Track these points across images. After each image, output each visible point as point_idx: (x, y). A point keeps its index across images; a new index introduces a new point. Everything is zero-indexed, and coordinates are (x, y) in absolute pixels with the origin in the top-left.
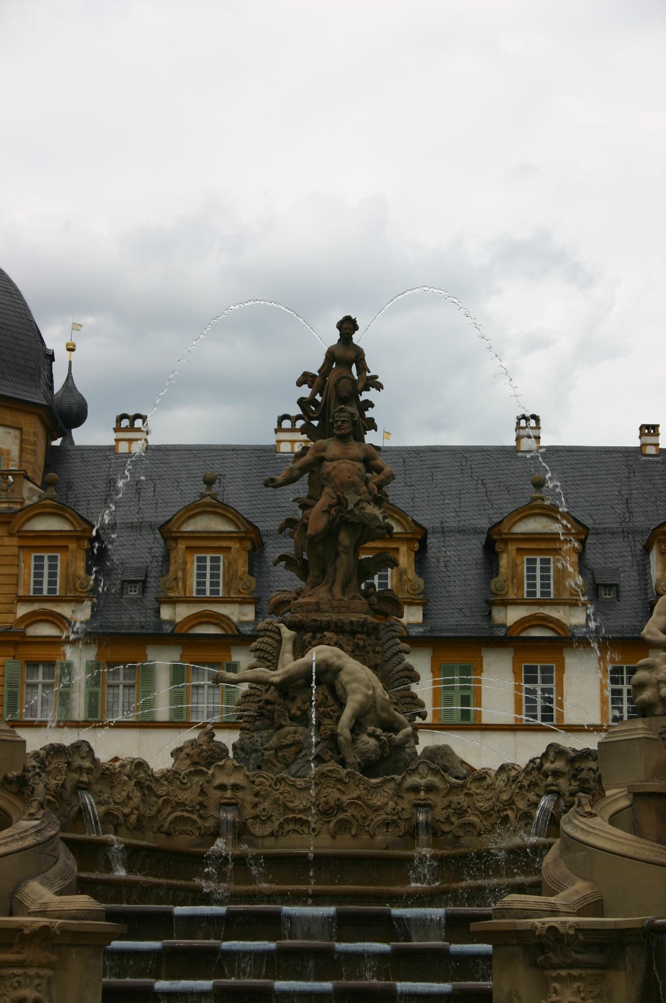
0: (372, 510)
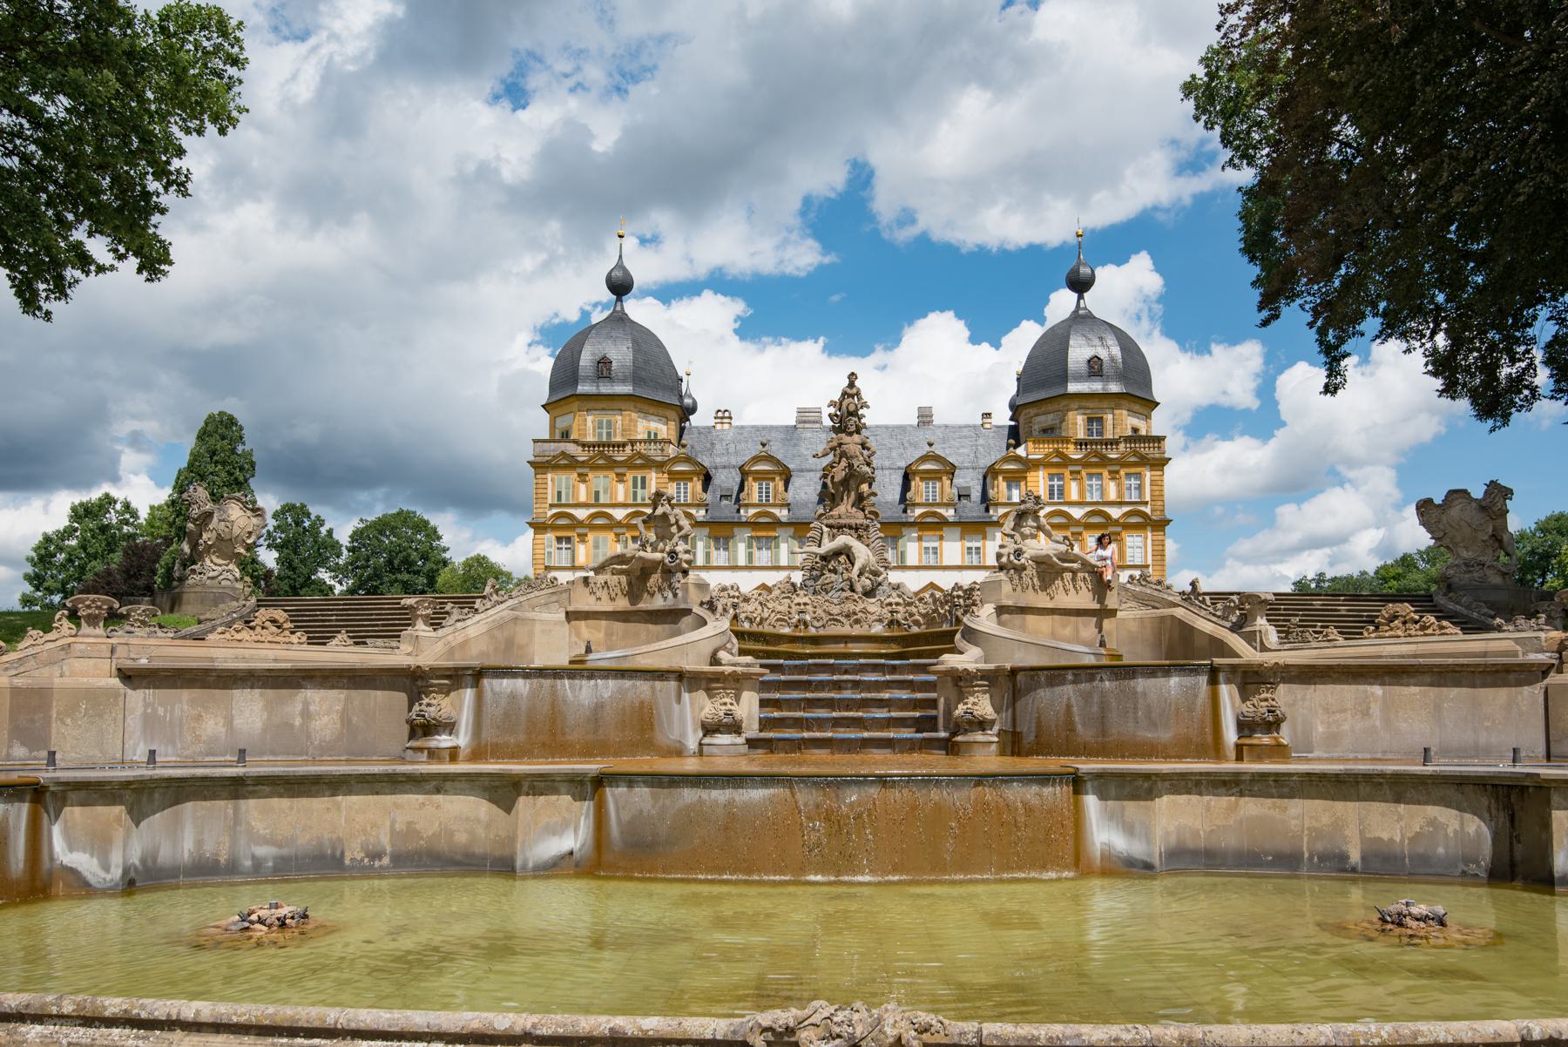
0: (866, 469)
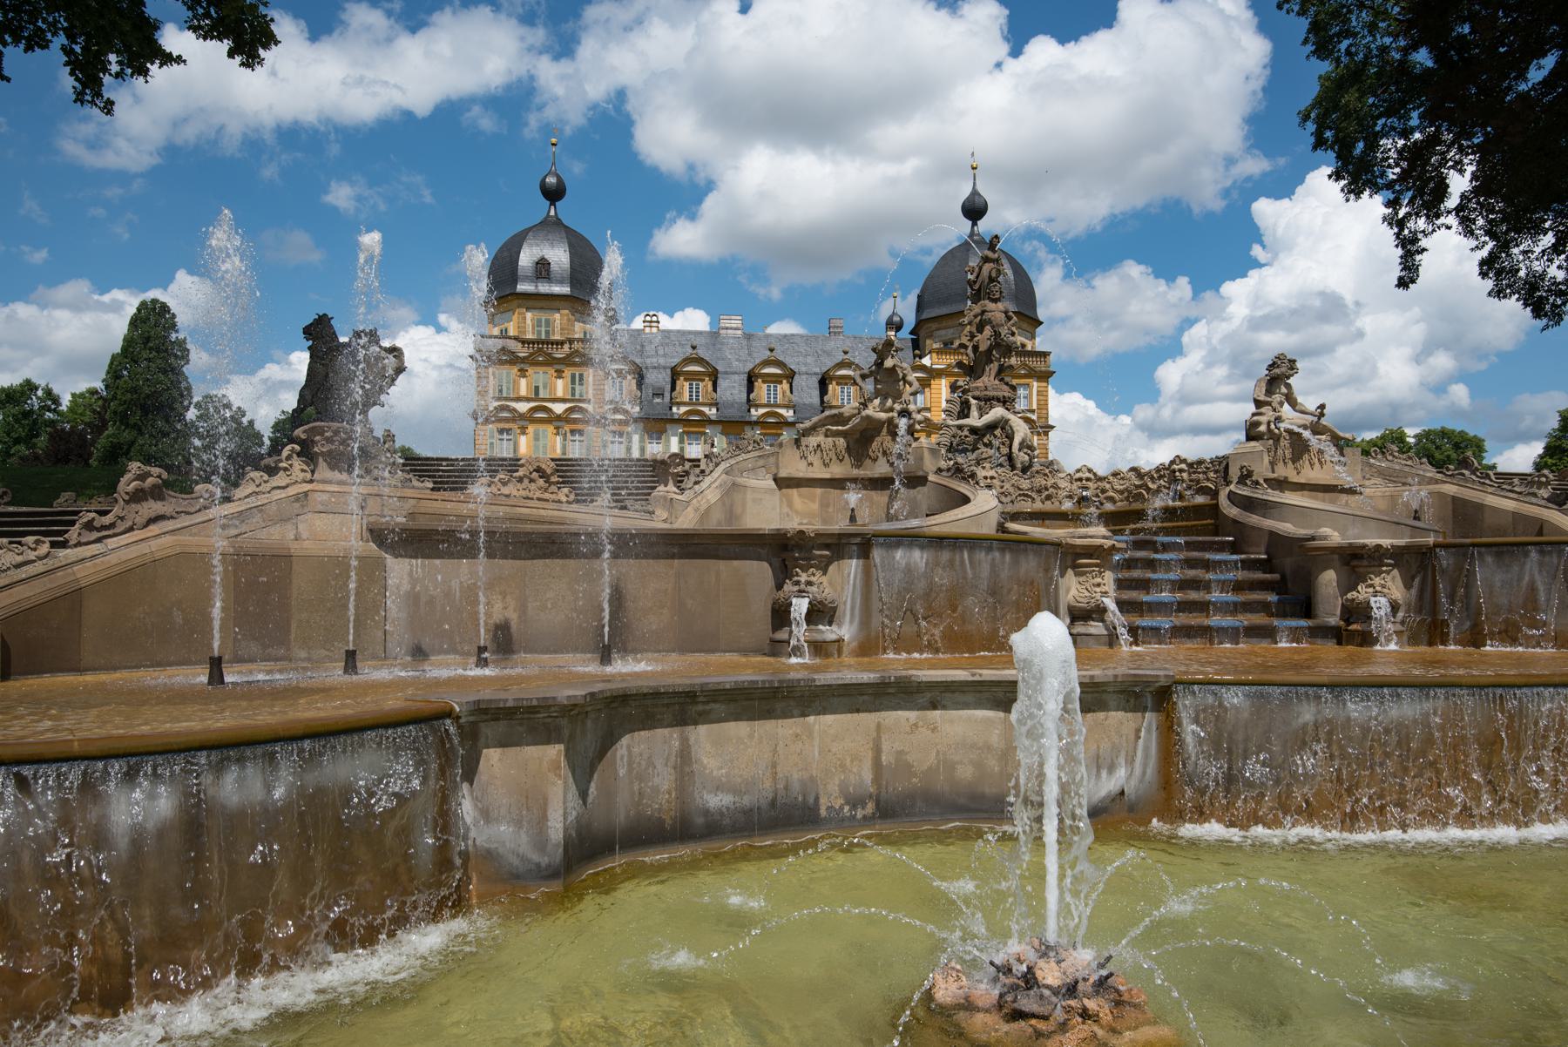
0: (1011, 338)
